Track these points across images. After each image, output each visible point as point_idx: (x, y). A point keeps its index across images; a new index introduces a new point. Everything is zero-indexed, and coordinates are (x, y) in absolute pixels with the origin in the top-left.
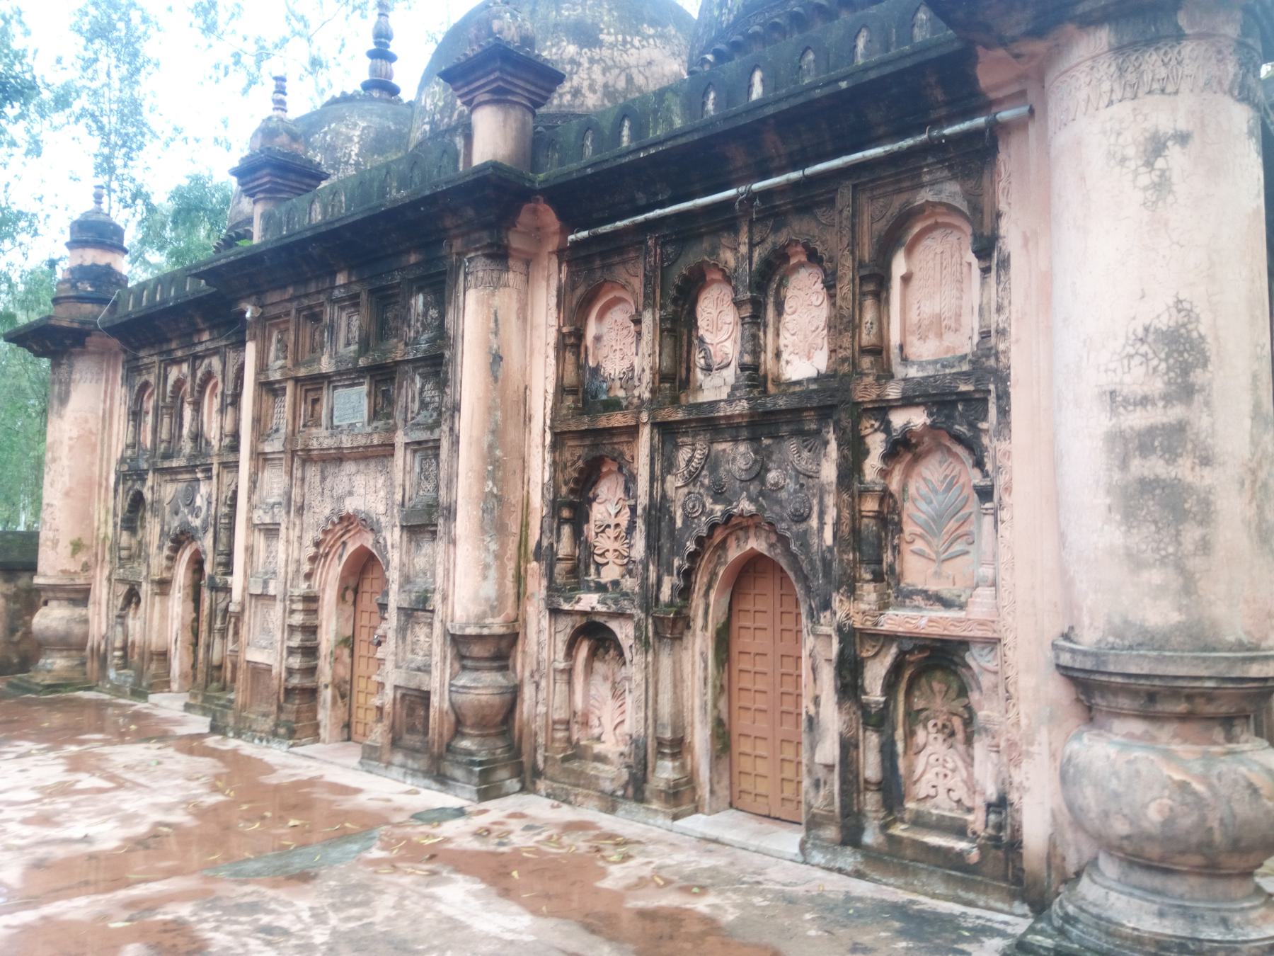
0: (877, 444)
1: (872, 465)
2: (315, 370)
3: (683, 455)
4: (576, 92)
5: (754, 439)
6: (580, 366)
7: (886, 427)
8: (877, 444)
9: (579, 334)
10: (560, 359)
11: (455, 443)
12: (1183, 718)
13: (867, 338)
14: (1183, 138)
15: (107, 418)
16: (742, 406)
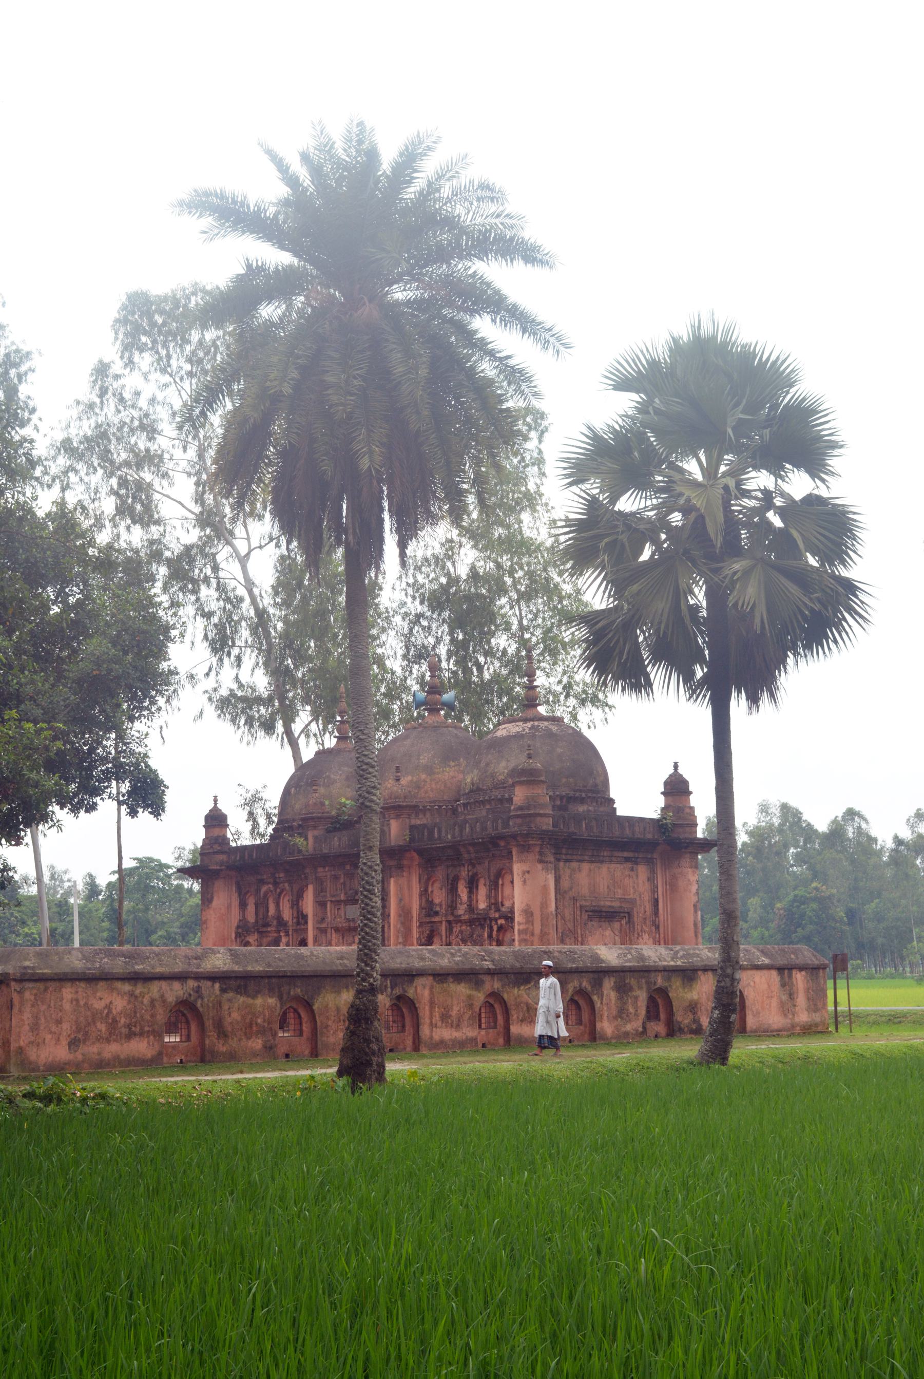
0: (495, 928)
1: (495, 933)
2: (338, 899)
3: (454, 930)
4: (426, 792)
5: (471, 926)
6: (427, 901)
7: (497, 923)
8: (495, 928)
9: (426, 890)
10: (421, 899)
11: (389, 926)
12: (789, 1036)
13: (493, 901)
14: (528, 872)
15: (229, 907)
16: (467, 917)
